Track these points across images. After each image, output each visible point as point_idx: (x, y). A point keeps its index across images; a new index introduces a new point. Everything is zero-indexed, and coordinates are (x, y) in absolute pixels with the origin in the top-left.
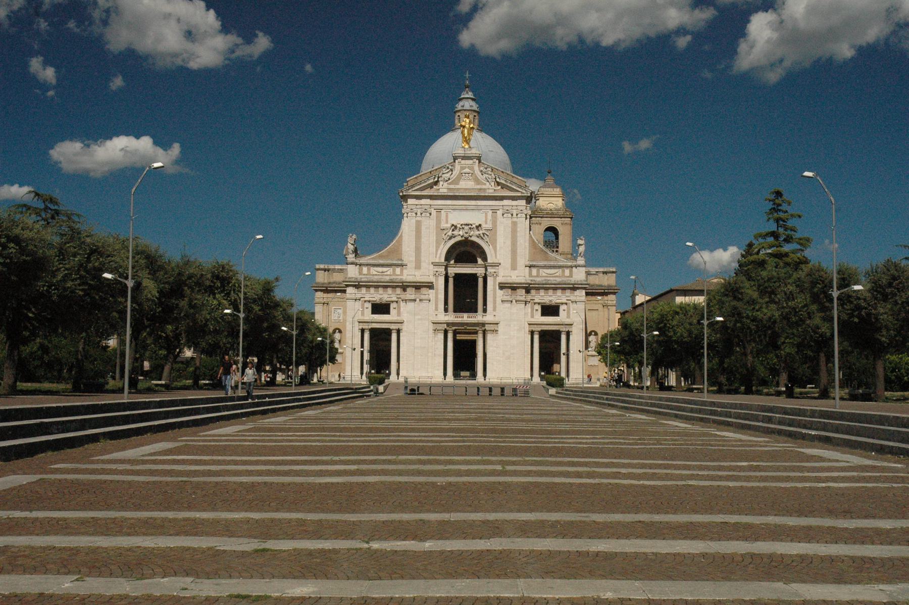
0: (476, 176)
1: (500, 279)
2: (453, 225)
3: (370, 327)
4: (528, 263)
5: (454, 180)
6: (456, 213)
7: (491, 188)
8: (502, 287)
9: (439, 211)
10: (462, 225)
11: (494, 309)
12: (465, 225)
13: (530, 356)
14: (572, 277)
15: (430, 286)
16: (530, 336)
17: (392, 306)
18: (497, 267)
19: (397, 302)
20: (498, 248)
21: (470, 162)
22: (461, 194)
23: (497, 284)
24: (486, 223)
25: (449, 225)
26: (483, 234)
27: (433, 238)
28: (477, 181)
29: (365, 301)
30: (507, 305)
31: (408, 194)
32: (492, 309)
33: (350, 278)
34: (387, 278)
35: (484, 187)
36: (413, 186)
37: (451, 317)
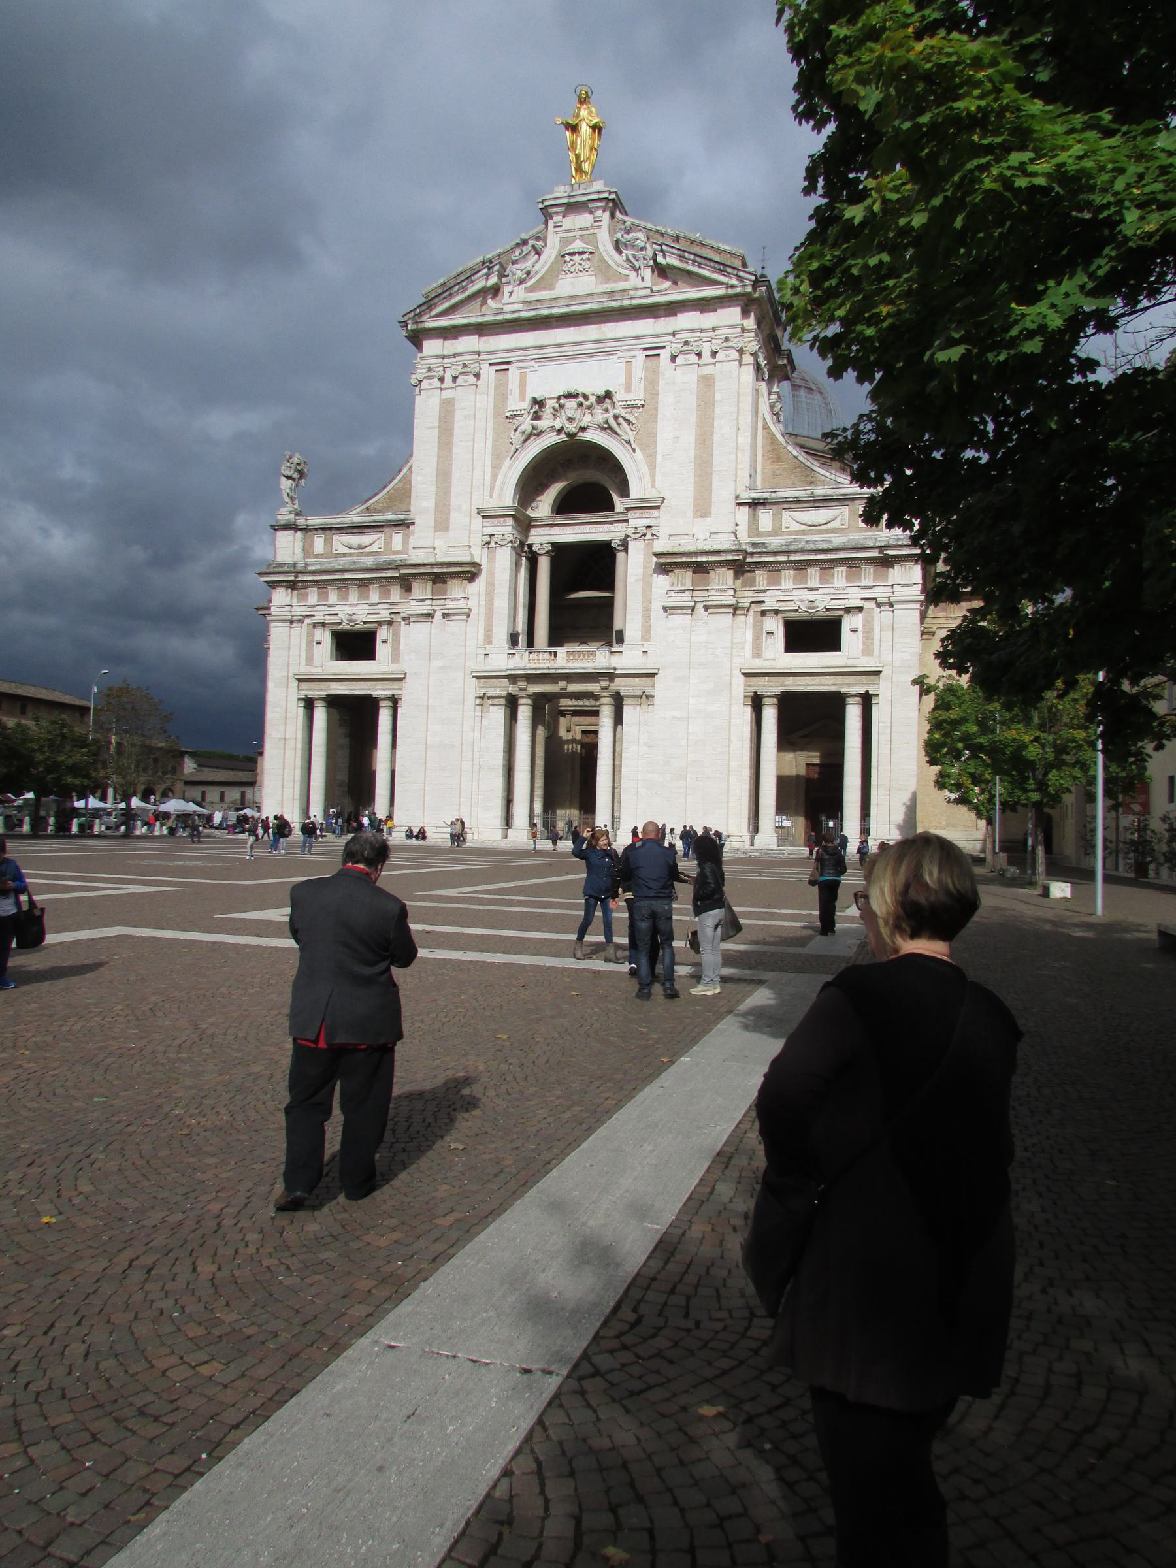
0: (603, 260)
1: (660, 546)
2: (535, 401)
3: (324, 693)
4: (745, 496)
5: (542, 278)
6: (549, 369)
7: (643, 285)
8: (666, 565)
9: (502, 367)
10: (559, 398)
11: (646, 636)
13: (746, 773)
16: (748, 711)
18: (655, 512)
19: (390, 623)
20: (659, 457)
21: (583, 220)
22: (555, 311)
24: (628, 388)
25: (526, 405)
26: (616, 417)
27: (485, 444)
28: (605, 272)
29: (314, 624)
31: (420, 326)
32: (639, 634)
33: (280, 565)
34: (369, 562)
35: (621, 286)
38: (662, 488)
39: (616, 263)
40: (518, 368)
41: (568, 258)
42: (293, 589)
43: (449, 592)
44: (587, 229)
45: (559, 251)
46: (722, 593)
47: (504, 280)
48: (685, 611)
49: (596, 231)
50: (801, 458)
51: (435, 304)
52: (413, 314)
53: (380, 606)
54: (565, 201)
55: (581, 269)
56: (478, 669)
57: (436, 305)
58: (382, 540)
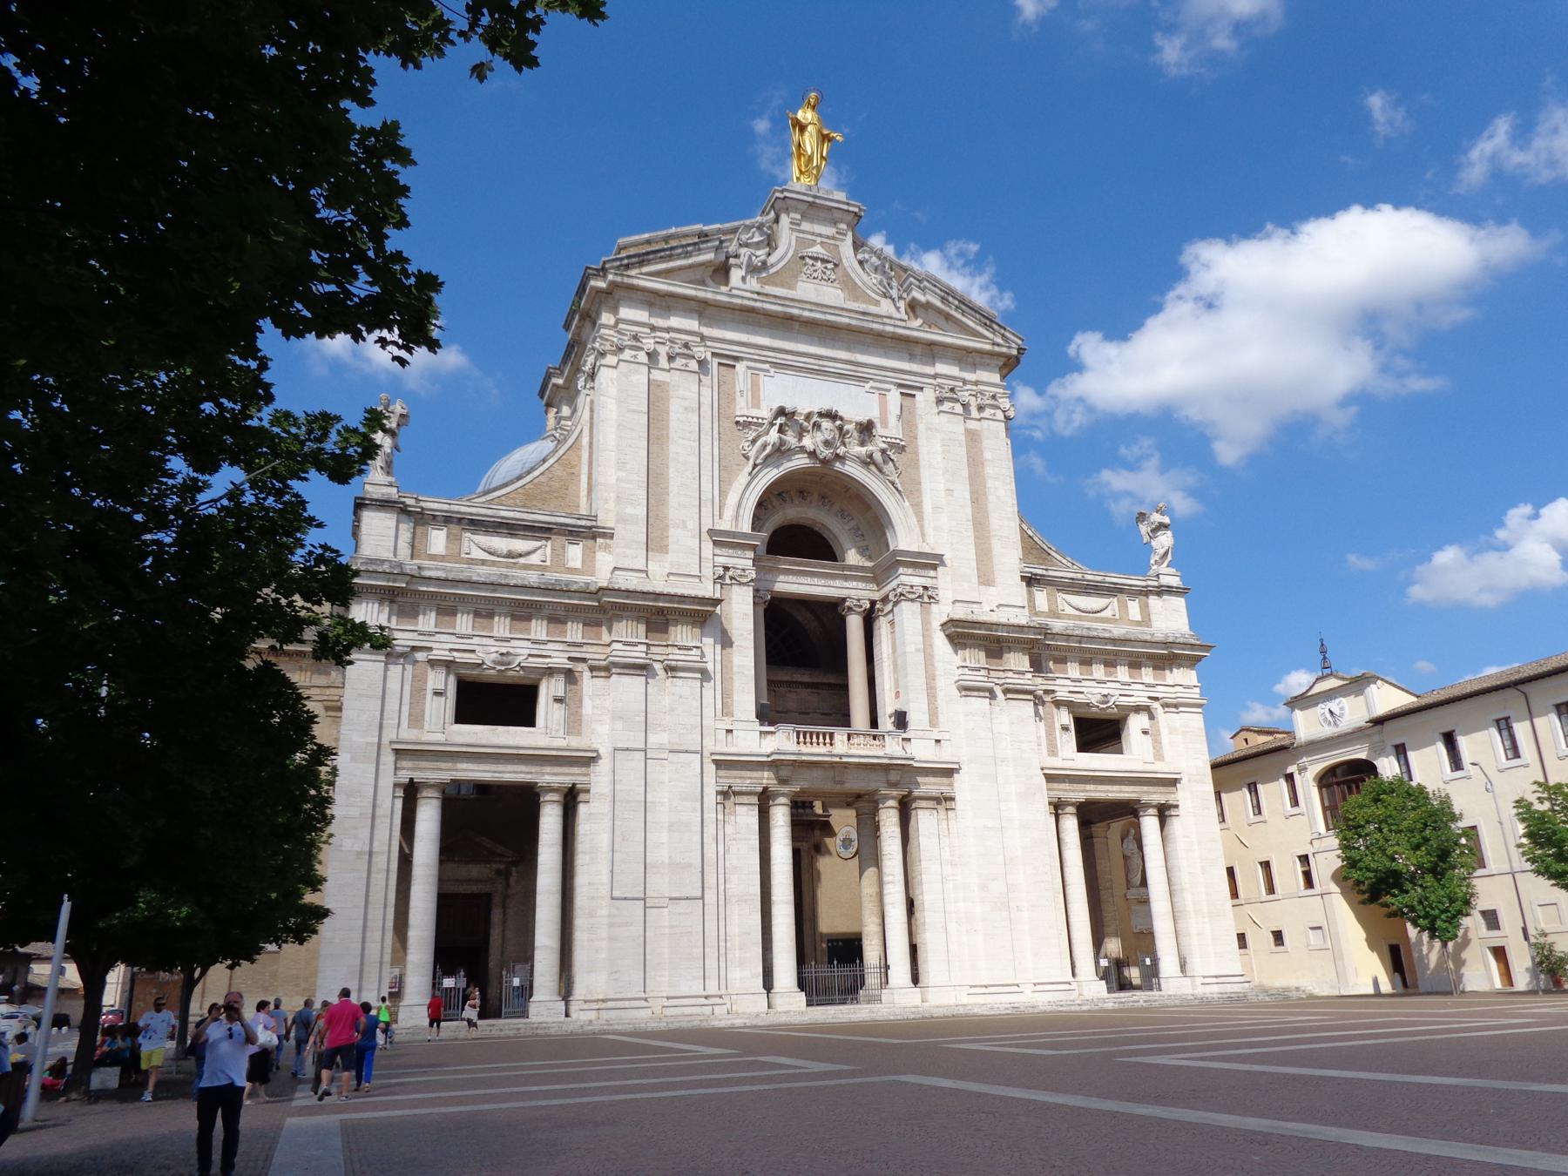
0: (848, 275)
2: (781, 412)
7: (898, 316)
8: (962, 634)
9: (729, 361)
10: (808, 417)
11: (933, 720)
12: (821, 415)
14: (1149, 626)
15: (702, 614)
17: (548, 691)
18: (932, 573)
20: (927, 508)
23: (936, 624)
25: (765, 413)
30: (980, 704)
31: (626, 280)
34: (532, 578)
35: (873, 309)
36: (643, 259)
37: (783, 741)
38: (933, 544)
39: (864, 283)
40: (749, 368)
41: (808, 260)
42: (392, 602)
43: (672, 637)
44: (828, 237)
45: (796, 251)
46: (1021, 676)
47: (732, 261)
48: (982, 694)
49: (838, 243)
50: (1036, 539)
51: (649, 261)
52: (618, 263)
53: (550, 646)
54: (810, 199)
55: (825, 277)
56: (718, 749)
57: (649, 262)
58: (548, 550)
